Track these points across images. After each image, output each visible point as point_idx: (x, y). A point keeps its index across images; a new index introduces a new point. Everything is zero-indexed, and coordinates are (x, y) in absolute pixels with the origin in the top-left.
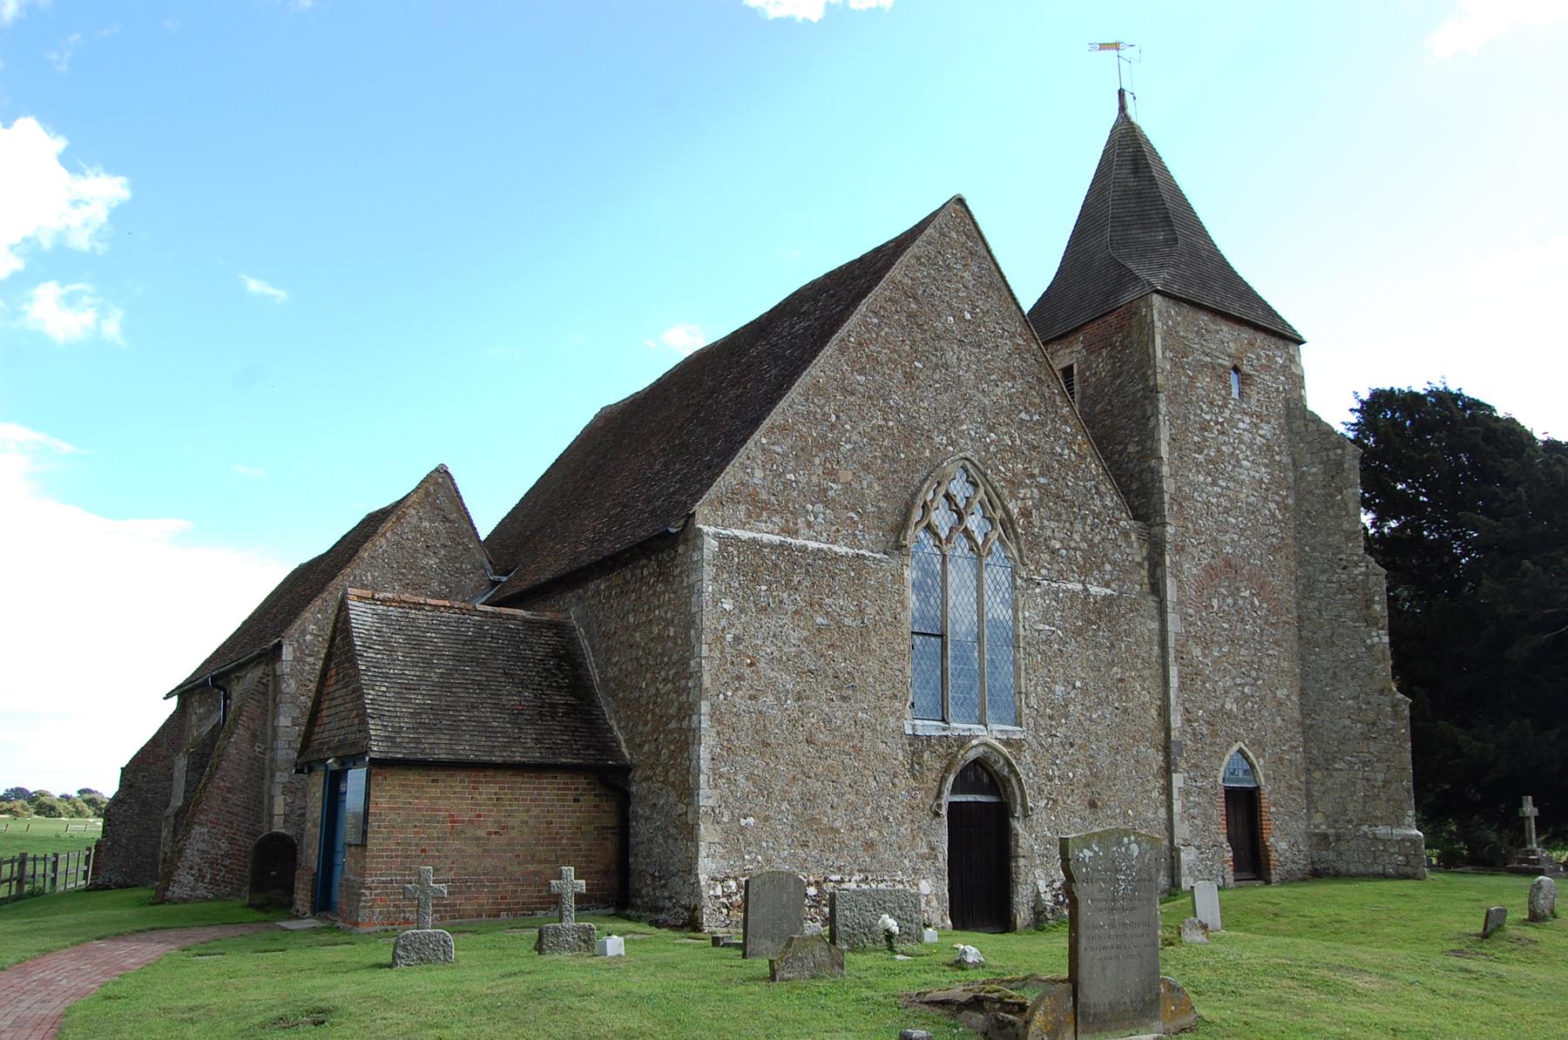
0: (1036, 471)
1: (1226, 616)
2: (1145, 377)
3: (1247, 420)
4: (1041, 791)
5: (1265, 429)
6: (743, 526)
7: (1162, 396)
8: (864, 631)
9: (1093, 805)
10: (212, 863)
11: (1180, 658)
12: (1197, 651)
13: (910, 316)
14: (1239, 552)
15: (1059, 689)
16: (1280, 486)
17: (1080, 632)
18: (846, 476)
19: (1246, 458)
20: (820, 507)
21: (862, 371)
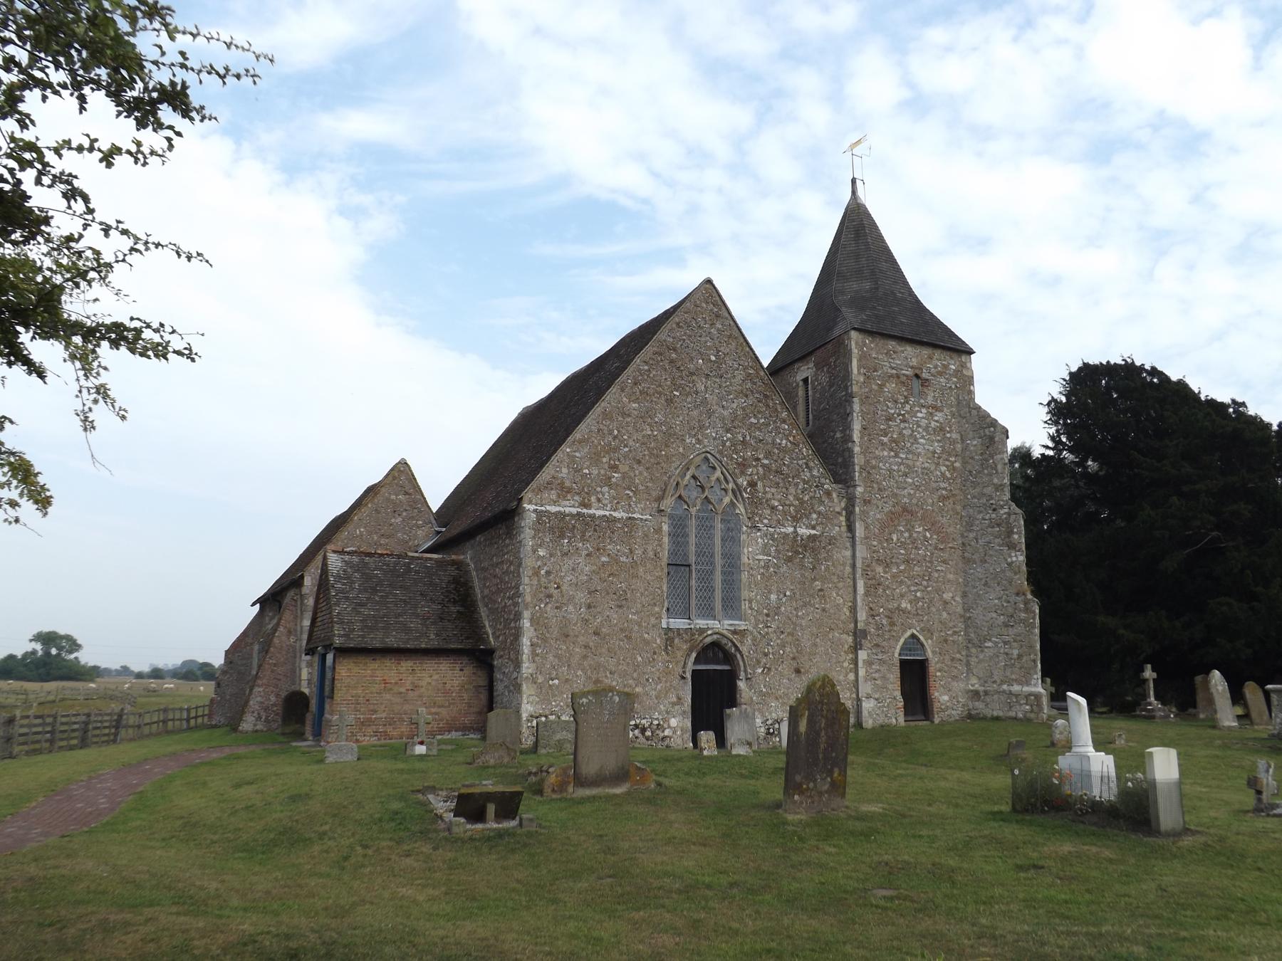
0: (761, 456)
2: (846, 388)
3: (924, 410)
4: (758, 662)
5: (939, 416)
6: (555, 503)
7: (856, 400)
8: (634, 564)
9: (798, 671)
10: (266, 709)
11: (865, 574)
13: (672, 361)
14: (914, 501)
15: (773, 597)
16: (950, 455)
17: (789, 560)
18: (624, 468)
19: (923, 437)
20: (606, 489)
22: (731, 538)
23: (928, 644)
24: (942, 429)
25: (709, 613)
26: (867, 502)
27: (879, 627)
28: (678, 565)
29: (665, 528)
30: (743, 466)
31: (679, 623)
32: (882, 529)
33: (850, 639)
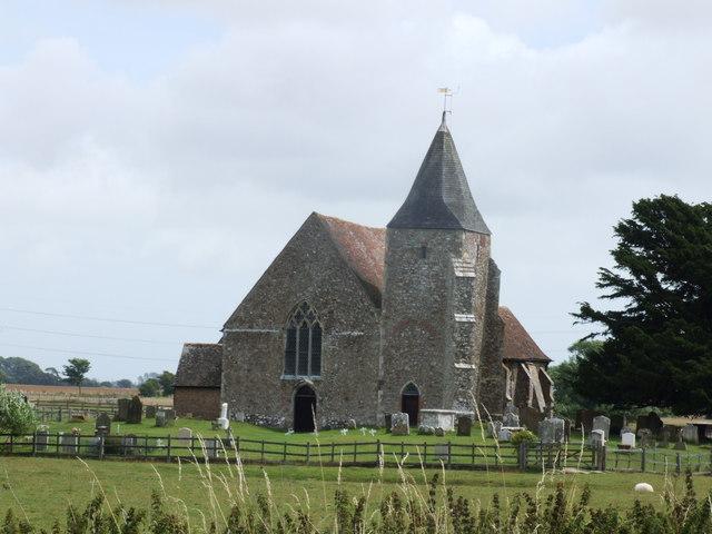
1: (408, 338)
5: (436, 268)
9: (347, 399)
25: (304, 371)
28: (290, 353)
30: (326, 303)
31: (289, 377)
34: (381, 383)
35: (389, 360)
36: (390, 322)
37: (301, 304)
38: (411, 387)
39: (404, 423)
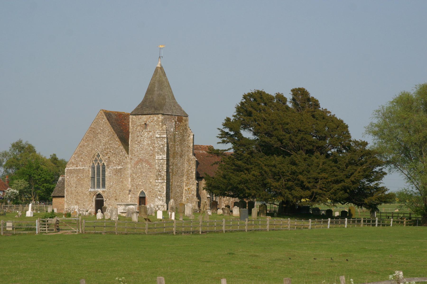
5: (151, 134)
8: (84, 178)
9: (116, 199)
12: (134, 175)
15: (111, 183)
17: (115, 174)
21: (86, 142)
22: (104, 171)
23: (146, 193)
24: (151, 137)
25: (98, 187)
26: (131, 159)
27: (134, 189)
29: (90, 170)
32: (135, 164)
33: (128, 192)
34: (130, 191)
35: (133, 179)
36: (133, 162)
37: (97, 154)
38: (142, 193)
39: (76, 210)
